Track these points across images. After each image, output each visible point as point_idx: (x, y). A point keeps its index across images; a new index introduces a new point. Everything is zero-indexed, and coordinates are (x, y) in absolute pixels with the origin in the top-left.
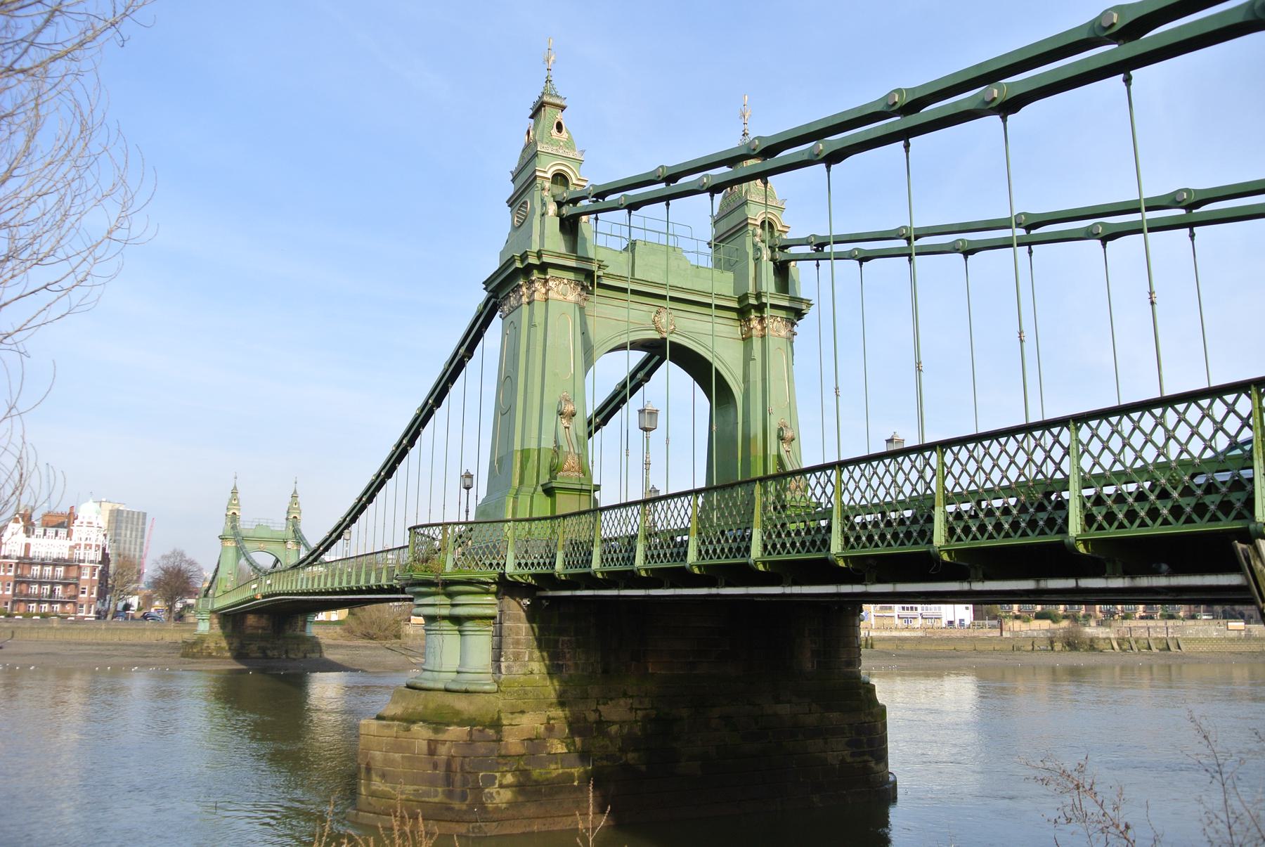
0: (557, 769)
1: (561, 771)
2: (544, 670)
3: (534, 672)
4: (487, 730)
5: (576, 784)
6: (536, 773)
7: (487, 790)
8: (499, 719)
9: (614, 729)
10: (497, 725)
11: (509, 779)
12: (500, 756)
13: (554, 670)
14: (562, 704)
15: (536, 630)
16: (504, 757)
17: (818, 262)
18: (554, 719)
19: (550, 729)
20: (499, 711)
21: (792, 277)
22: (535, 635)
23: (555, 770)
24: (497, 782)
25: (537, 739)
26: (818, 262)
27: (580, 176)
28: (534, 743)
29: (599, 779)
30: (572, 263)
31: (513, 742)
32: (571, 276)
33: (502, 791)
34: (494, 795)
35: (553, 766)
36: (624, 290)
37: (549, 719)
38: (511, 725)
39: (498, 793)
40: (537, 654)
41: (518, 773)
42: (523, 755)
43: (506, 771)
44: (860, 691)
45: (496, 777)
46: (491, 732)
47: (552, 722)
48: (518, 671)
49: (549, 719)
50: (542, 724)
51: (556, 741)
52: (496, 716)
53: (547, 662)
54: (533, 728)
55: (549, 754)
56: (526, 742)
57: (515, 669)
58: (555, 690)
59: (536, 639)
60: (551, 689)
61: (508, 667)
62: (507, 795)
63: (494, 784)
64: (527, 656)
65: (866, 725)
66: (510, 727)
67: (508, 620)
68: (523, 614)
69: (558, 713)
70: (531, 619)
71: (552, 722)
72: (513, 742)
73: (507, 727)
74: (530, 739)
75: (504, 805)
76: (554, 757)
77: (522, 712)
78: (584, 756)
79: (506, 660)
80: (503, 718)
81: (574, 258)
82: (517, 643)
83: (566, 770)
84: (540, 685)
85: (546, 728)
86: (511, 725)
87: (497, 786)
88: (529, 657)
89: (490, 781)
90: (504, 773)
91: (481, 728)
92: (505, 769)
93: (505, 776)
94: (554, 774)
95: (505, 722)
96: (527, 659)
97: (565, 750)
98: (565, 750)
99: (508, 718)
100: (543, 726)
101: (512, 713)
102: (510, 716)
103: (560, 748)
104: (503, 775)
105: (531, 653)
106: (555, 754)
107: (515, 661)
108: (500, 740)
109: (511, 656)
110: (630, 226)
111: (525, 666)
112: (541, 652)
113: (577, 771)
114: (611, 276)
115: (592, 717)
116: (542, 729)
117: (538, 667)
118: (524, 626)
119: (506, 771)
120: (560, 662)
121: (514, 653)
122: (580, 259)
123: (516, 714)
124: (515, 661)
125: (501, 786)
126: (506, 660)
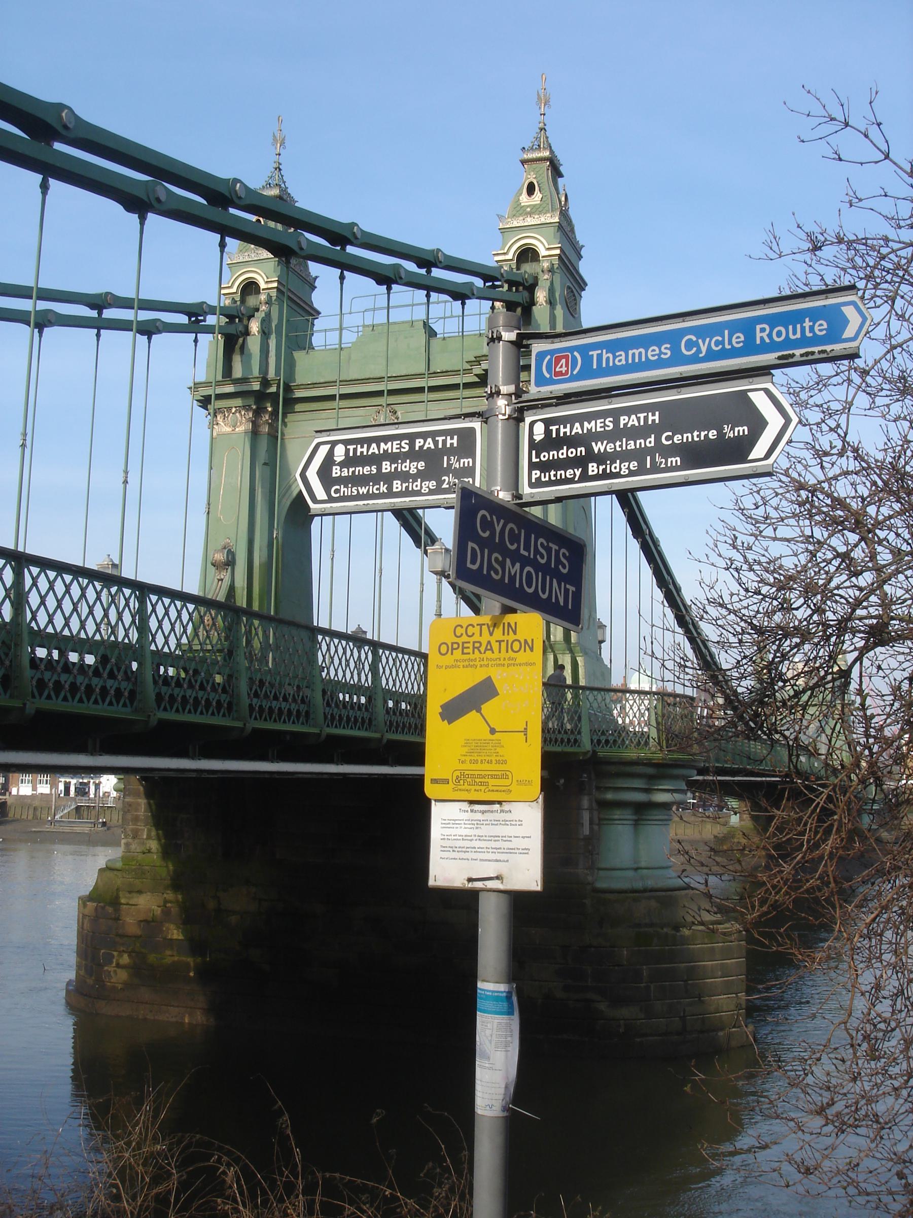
0: (173, 956)
1: (176, 958)
2: (160, 850)
3: (152, 851)
4: (107, 907)
5: (192, 974)
6: (152, 958)
7: (106, 968)
8: (117, 897)
9: (234, 919)
10: (115, 903)
11: (125, 959)
12: (118, 935)
13: (167, 852)
14: (176, 884)
15: (154, 807)
16: (122, 936)
17: (493, 304)
18: (171, 902)
19: (166, 912)
20: (117, 889)
21: (537, 321)
22: (151, 811)
23: (170, 957)
24: (114, 960)
25: (153, 921)
26: (493, 304)
27: (268, 278)
28: (151, 924)
29: (206, 974)
30: (230, 389)
31: (130, 923)
32: (238, 402)
33: (119, 971)
34: (112, 973)
35: (168, 952)
36: (332, 398)
37: (166, 901)
38: (127, 904)
39: (115, 972)
40: (154, 833)
41: (134, 954)
42: (141, 936)
43: (124, 951)
44: (584, 901)
45: (113, 956)
46: (110, 910)
47: (169, 905)
48: (136, 849)
49: (166, 901)
50: (158, 906)
51: (172, 926)
52: (115, 894)
53: (163, 841)
54: (150, 910)
55: (165, 939)
56: (142, 924)
57: (133, 847)
58: (168, 871)
59: (153, 816)
60: (166, 870)
61: (127, 845)
62: (123, 975)
63: (112, 962)
64: (145, 833)
65: (593, 949)
66: (127, 907)
67: (129, 795)
68: (142, 789)
69: (170, 895)
70: (149, 795)
71: (169, 905)
72: (130, 923)
73: (125, 906)
74: (145, 921)
75: (120, 986)
76: (171, 943)
77: (140, 892)
78: (196, 946)
79: (126, 837)
80: (121, 895)
81: (230, 382)
82: (136, 819)
83: (184, 959)
84: (158, 864)
85: (162, 911)
86: (127, 904)
87: (114, 964)
88: (147, 835)
89: (109, 959)
90: (121, 953)
91: (102, 904)
92: (122, 949)
93: (122, 956)
94: (168, 960)
95: (123, 901)
96: (145, 837)
97: (181, 937)
98: (181, 937)
99: (126, 897)
100: (160, 909)
101: (130, 892)
102: (128, 895)
103: (176, 934)
104: (120, 956)
105: (149, 831)
106: (171, 940)
107: (134, 838)
108: (117, 919)
109: (130, 833)
110: (413, 305)
111: (143, 844)
112: (157, 830)
113: (190, 960)
114: (302, 387)
115: (212, 905)
116: (159, 912)
117: (154, 845)
118: (143, 802)
119: (124, 951)
120: (179, 842)
121: (132, 830)
122: (236, 382)
123: (134, 895)
124: (134, 838)
125: (118, 966)
126: (126, 837)
